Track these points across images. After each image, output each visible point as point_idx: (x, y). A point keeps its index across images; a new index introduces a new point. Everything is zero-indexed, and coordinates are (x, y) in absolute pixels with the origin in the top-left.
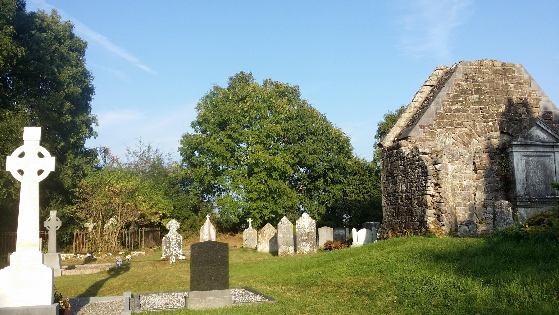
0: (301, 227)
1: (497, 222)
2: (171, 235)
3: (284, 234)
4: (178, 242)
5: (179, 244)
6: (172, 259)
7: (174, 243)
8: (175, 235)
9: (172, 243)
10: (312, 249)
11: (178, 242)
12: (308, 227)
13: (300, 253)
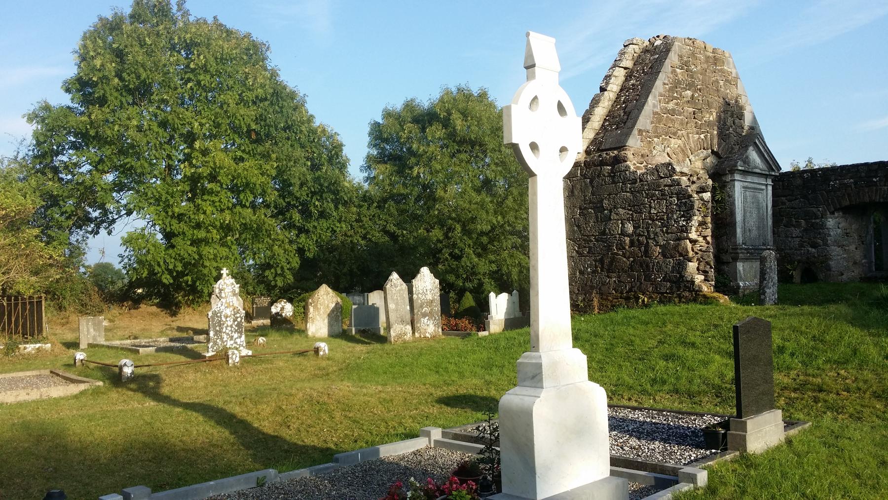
0: (421, 292)
1: (766, 282)
2: (223, 307)
3: (397, 304)
4: (236, 323)
5: (239, 325)
6: (234, 356)
7: (229, 323)
8: (231, 309)
9: (225, 325)
10: (437, 329)
11: (236, 323)
12: (430, 292)
13: (420, 337)
